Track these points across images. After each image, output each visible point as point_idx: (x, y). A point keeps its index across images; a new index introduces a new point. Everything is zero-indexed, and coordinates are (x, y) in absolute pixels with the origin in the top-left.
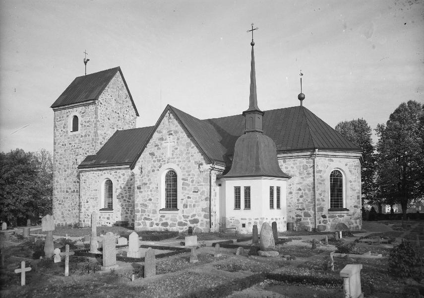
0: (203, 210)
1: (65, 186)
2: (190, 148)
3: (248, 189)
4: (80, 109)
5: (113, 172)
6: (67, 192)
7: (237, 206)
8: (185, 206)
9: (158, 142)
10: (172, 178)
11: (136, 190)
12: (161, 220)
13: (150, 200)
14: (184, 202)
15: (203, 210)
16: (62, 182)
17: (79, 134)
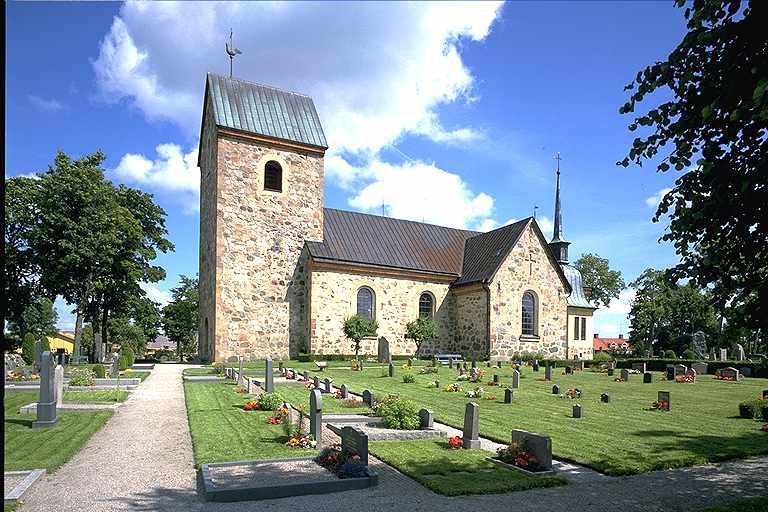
0: (562, 338)
1: (250, 288)
2: (551, 273)
3: (584, 320)
4: (288, 154)
5: (377, 279)
6: (254, 298)
7: (576, 338)
8: (546, 334)
9: (518, 257)
10: (530, 298)
11: (492, 310)
12: (521, 348)
13: (509, 324)
14: (544, 328)
15: (562, 338)
16: (243, 279)
17: (284, 198)
